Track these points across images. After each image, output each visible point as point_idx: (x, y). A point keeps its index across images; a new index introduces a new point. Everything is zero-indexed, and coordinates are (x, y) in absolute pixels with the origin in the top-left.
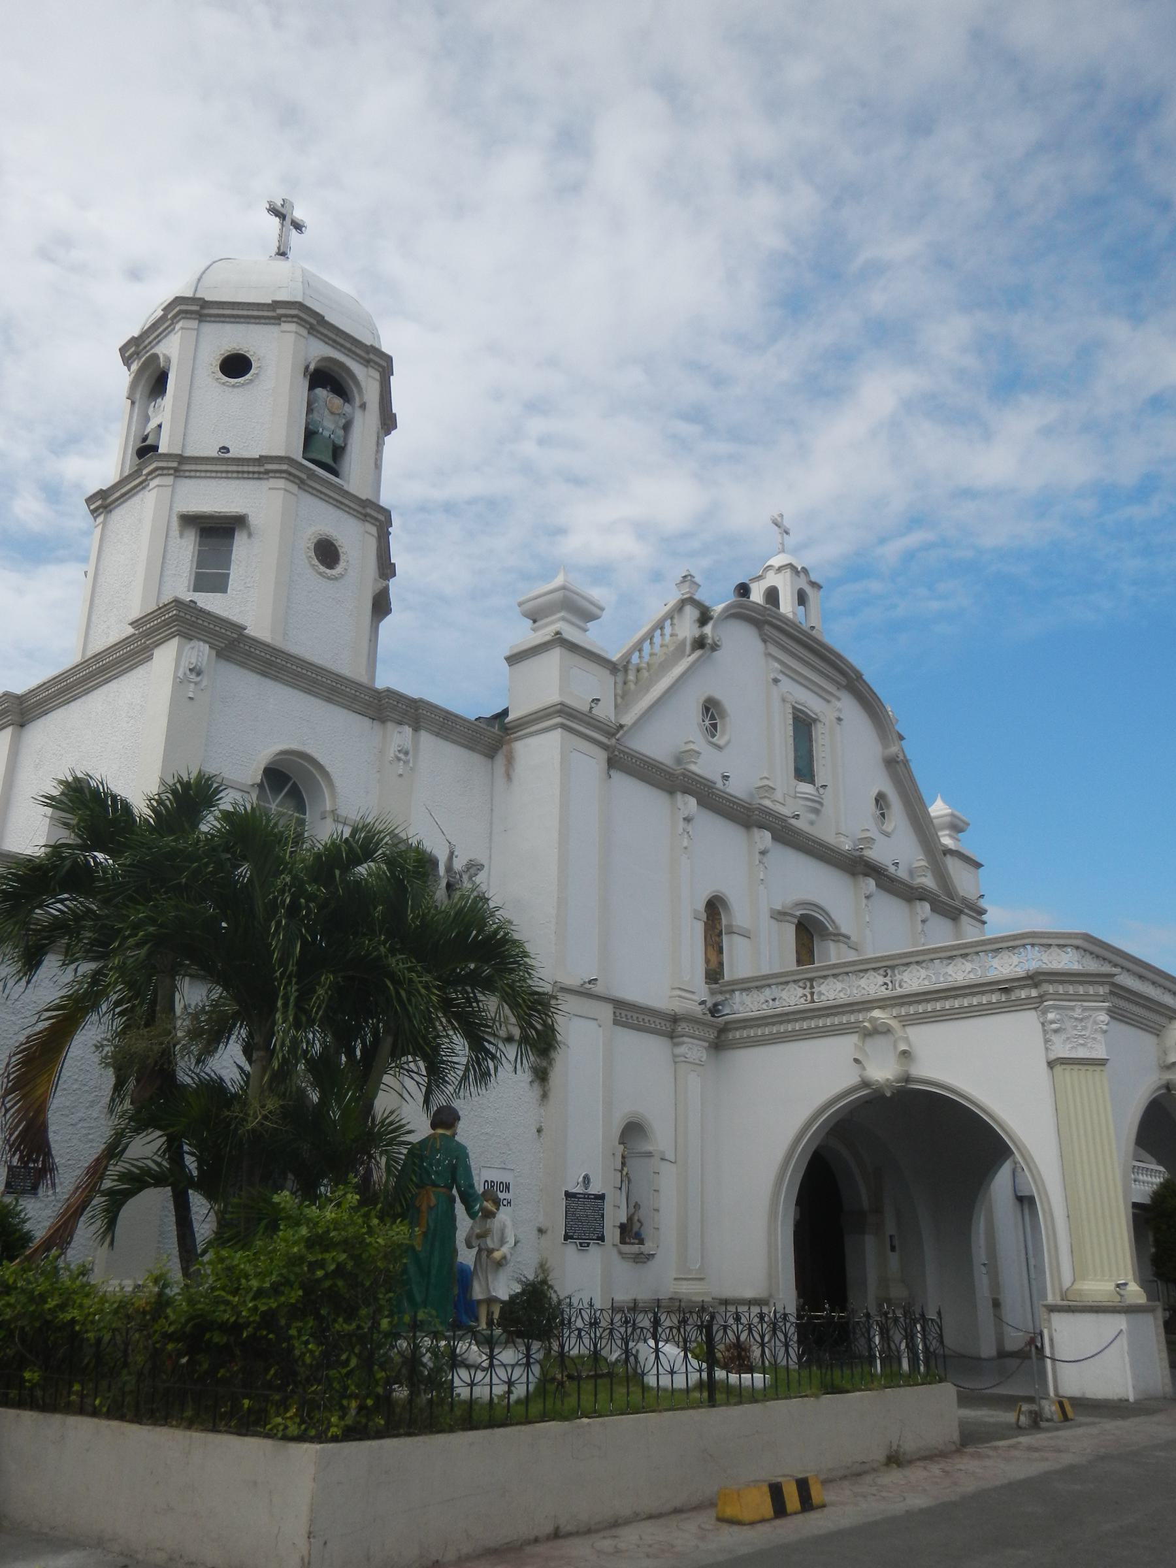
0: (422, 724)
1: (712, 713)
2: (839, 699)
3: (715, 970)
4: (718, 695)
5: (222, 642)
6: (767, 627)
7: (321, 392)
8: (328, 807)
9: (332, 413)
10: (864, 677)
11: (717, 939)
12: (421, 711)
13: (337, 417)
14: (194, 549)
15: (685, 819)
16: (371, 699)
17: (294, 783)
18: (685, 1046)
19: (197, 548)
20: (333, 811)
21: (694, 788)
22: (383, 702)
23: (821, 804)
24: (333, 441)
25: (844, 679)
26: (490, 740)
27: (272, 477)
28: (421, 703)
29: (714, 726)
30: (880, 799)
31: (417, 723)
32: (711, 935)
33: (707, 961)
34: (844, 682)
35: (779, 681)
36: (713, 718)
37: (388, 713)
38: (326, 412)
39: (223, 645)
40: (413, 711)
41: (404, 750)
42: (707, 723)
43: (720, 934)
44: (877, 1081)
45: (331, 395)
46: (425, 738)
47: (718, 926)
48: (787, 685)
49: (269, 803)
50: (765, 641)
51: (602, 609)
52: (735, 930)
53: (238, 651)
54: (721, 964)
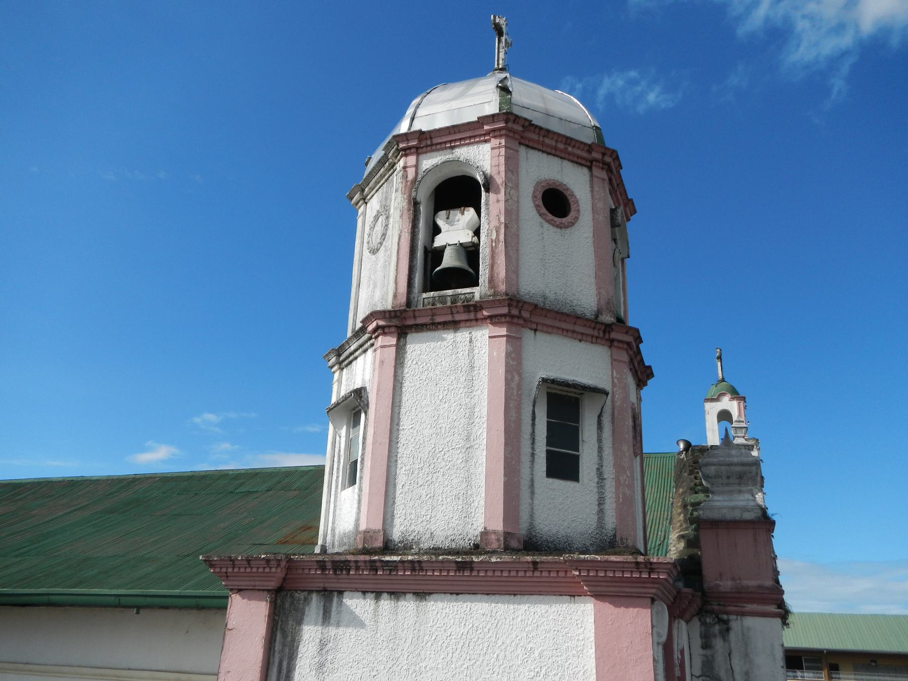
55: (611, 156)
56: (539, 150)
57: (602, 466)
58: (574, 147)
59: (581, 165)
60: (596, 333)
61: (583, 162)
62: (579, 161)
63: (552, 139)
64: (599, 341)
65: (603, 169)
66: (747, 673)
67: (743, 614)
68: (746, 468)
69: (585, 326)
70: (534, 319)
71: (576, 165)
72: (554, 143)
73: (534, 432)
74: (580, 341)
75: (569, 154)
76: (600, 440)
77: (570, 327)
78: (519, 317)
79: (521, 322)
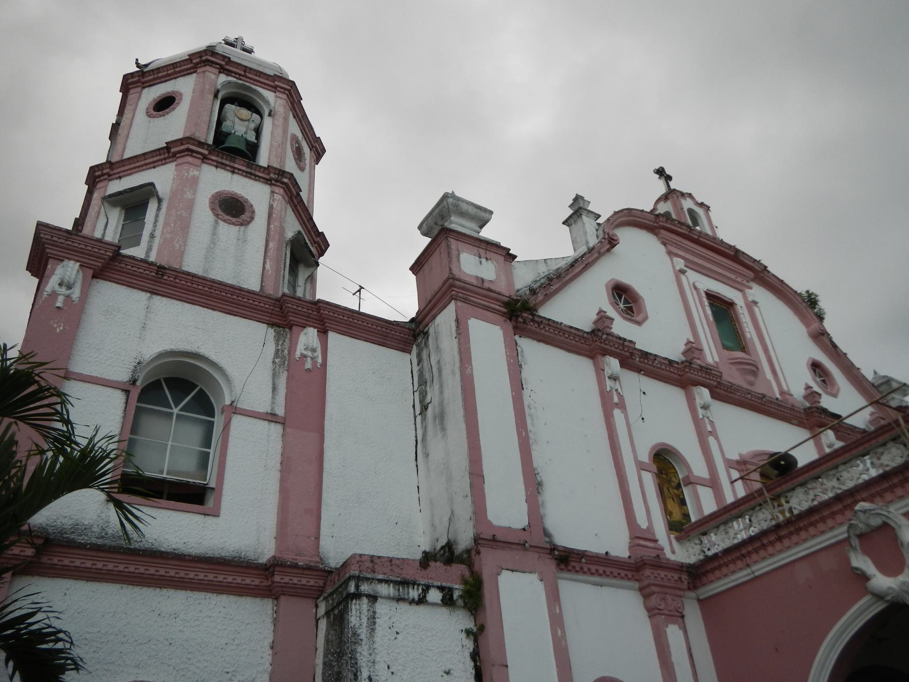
0: (327, 324)
1: (625, 298)
2: (751, 288)
3: (680, 522)
4: (626, 279)
5: (100, 262)
6: (663, 231)
7: (228, 106)
8: (228, 402)
9: (242, 120)
10: (768, 269)
11: (676, 491)
12: (322, 311)
13: (246, 123)
14: (118, 223)
15: (609, 378)
16: (272, 307)
17: (201, 390)
18: (655, 596)
19: (122, 222)
20: (231, 404)
21: (613, 349)
22: (284, 308)
23: (757, 368)
24: (246, 139)
25: (751, 273)
26: (402, 335)
27: (179, 157)
28: (321, 304)
29: (630, 309)
30: (816, 366)
31: (323, 325)
32: (668, 488)
33: (667, 512)
34: (751, 275)
35: (686, 271)
36: (626, 302)
37: (291, 318)
38: (237, 120)
39: (100, 264)
40: (315, 313)
41: (310, 347)
42: (622, 306)
43: (679, 486)
44: (890, 588)
45: (238, 108)
46: (334, 338)
47: (674, 479)
48: (693, 276)
49: (172, 408)
50: (664, 244)
51: (491, 213)
52: (692, 481)
53: (114, 270)
54: (686, 516)
55: (206, 55)
56: (158, 83)
57: (154, 231)
58: (181, 66)
59: (191, 73)
60: (162, 157)
61: (192, 70)
62: (189, 72)
63: (164, 71)
64: (167, 161)
65: (205, 66)
66: (439, 362)
67: (434, 317)
68: (440, 206)
69: (153, 157)
70: (115, 171)
71: (187, 76)
72: (165, 73)
73: (105, 232)
74: (154, 167)
75: (180, 72)
76: (157, 216)
77: (142, 163)
78: (103, 175)
79: (106, 177)
